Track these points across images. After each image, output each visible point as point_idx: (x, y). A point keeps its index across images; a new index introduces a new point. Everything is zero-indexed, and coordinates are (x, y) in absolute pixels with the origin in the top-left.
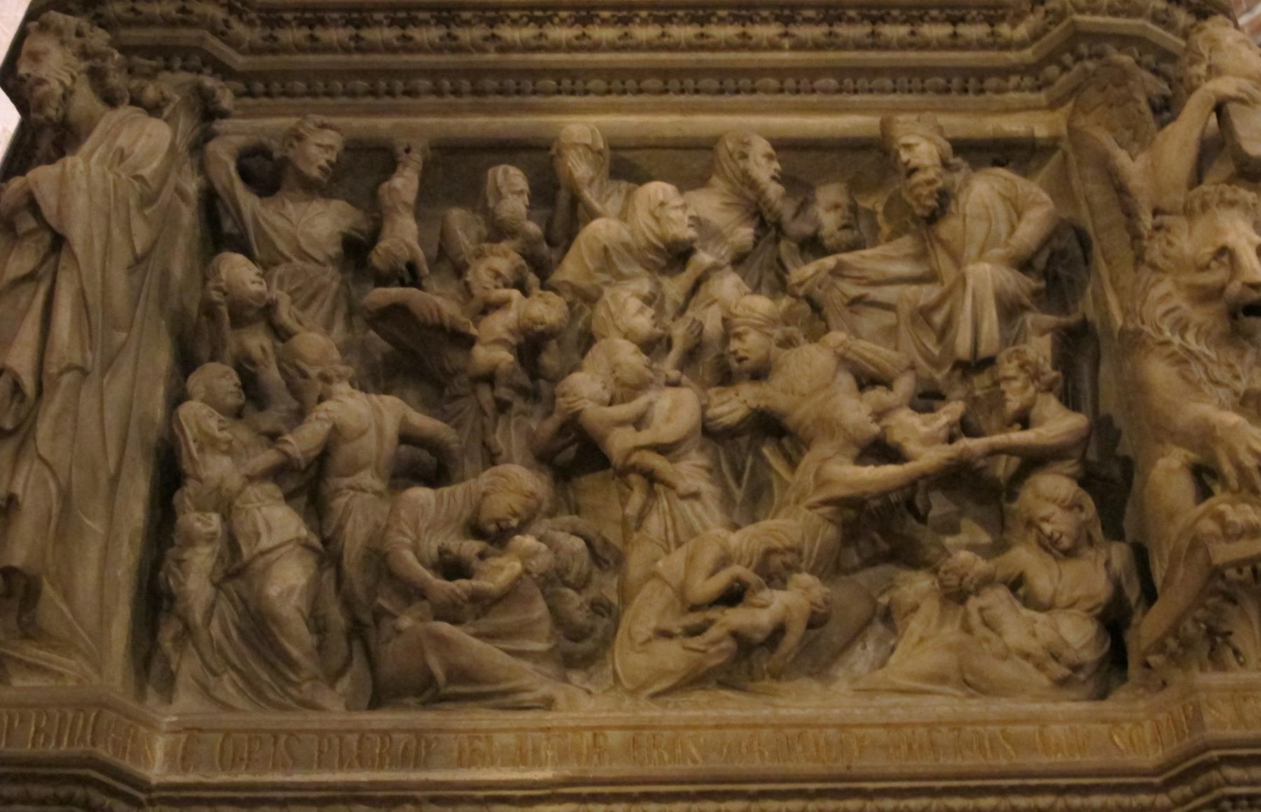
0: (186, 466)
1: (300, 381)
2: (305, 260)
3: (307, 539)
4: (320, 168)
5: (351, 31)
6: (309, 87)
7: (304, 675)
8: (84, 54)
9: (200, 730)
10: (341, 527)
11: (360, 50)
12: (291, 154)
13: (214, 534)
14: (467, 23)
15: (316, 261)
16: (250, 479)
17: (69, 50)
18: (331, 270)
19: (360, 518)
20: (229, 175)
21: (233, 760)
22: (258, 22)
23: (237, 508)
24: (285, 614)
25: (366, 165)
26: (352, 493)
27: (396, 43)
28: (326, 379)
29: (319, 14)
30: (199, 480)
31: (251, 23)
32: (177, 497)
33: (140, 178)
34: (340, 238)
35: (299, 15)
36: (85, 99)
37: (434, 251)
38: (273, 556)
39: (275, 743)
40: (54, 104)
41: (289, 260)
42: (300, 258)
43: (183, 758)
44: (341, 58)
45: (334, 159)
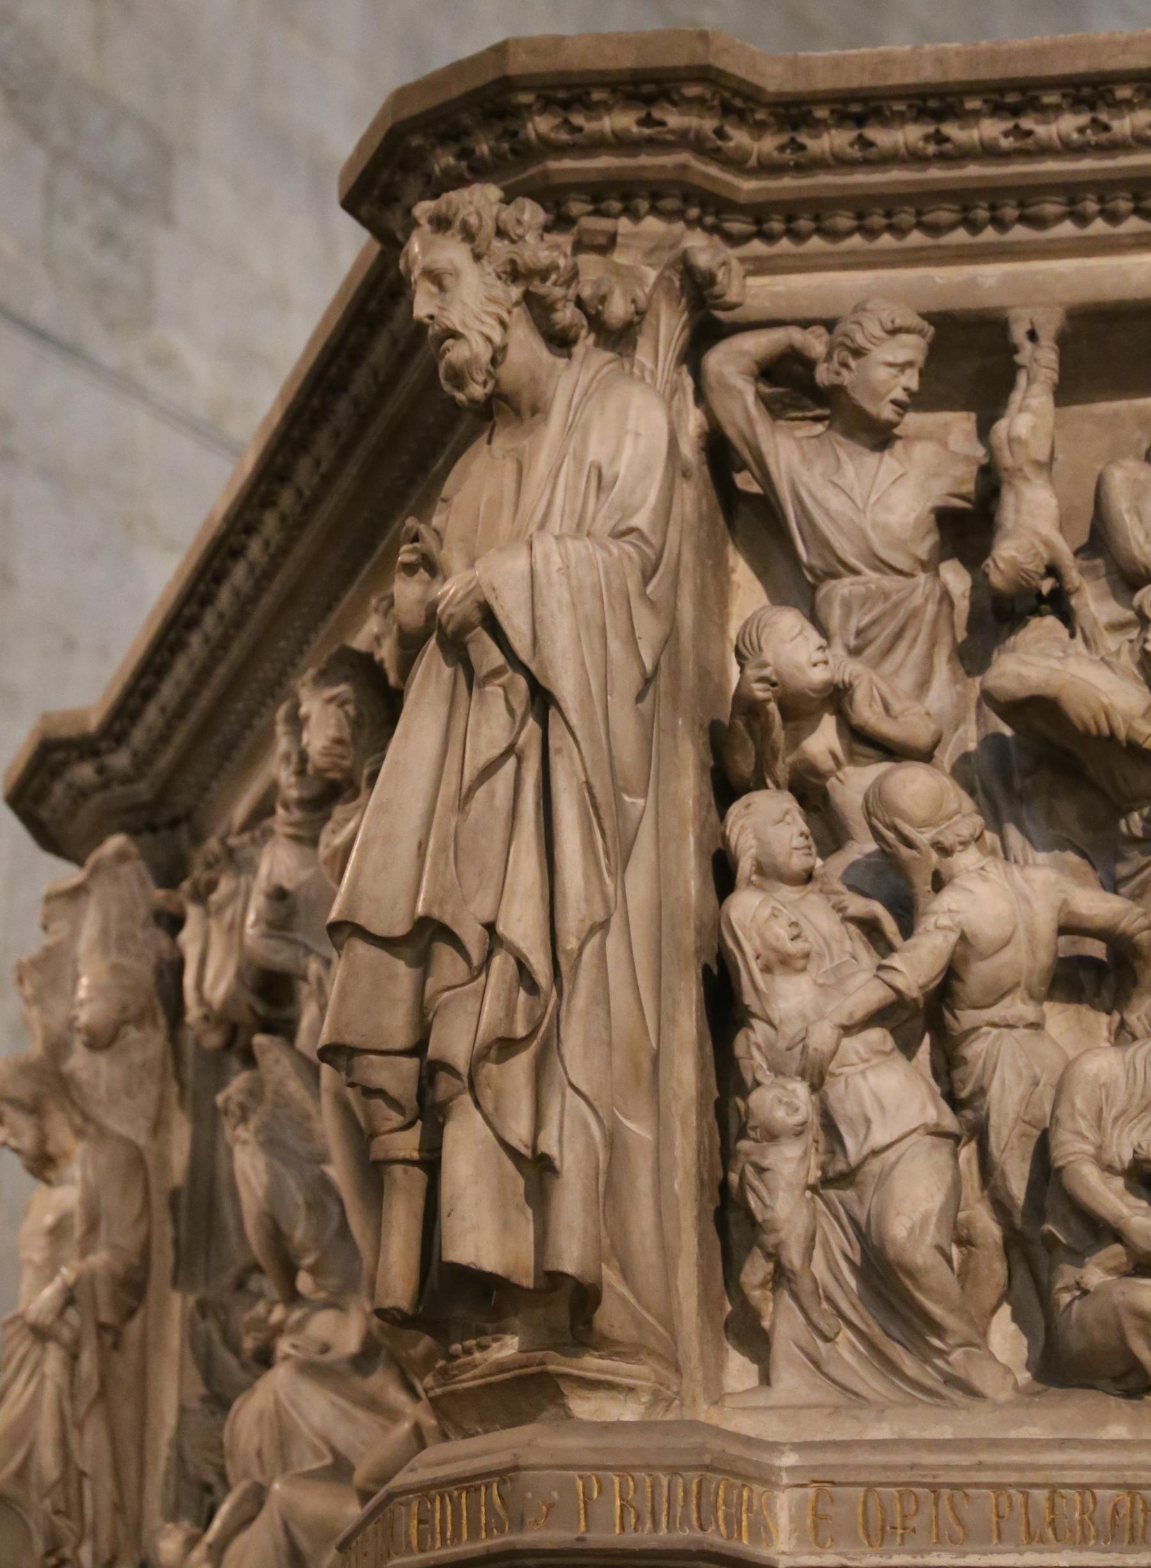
2: (884, 573)
4: (894, 402)
7: (951, 1341)
9: (833, 1483)
12: (846, 378)
13: (804, 1124)
15: (900, 572)
16: (848, 1030)
17: (489, 269)
19: (1010, 1077)
20: (746, 410)
21: (883, 1529)
23: (833, 1075)
24: (920, 1260)
28: (945, 851)
30: (770, 1022)
34: (932, 517)
37: (1084, 539)
38: (891, 1155)
39: (936, 1504)
41: (855, 572)
42: (875, 569)
43: (816, 1527)
45: (914, 385)
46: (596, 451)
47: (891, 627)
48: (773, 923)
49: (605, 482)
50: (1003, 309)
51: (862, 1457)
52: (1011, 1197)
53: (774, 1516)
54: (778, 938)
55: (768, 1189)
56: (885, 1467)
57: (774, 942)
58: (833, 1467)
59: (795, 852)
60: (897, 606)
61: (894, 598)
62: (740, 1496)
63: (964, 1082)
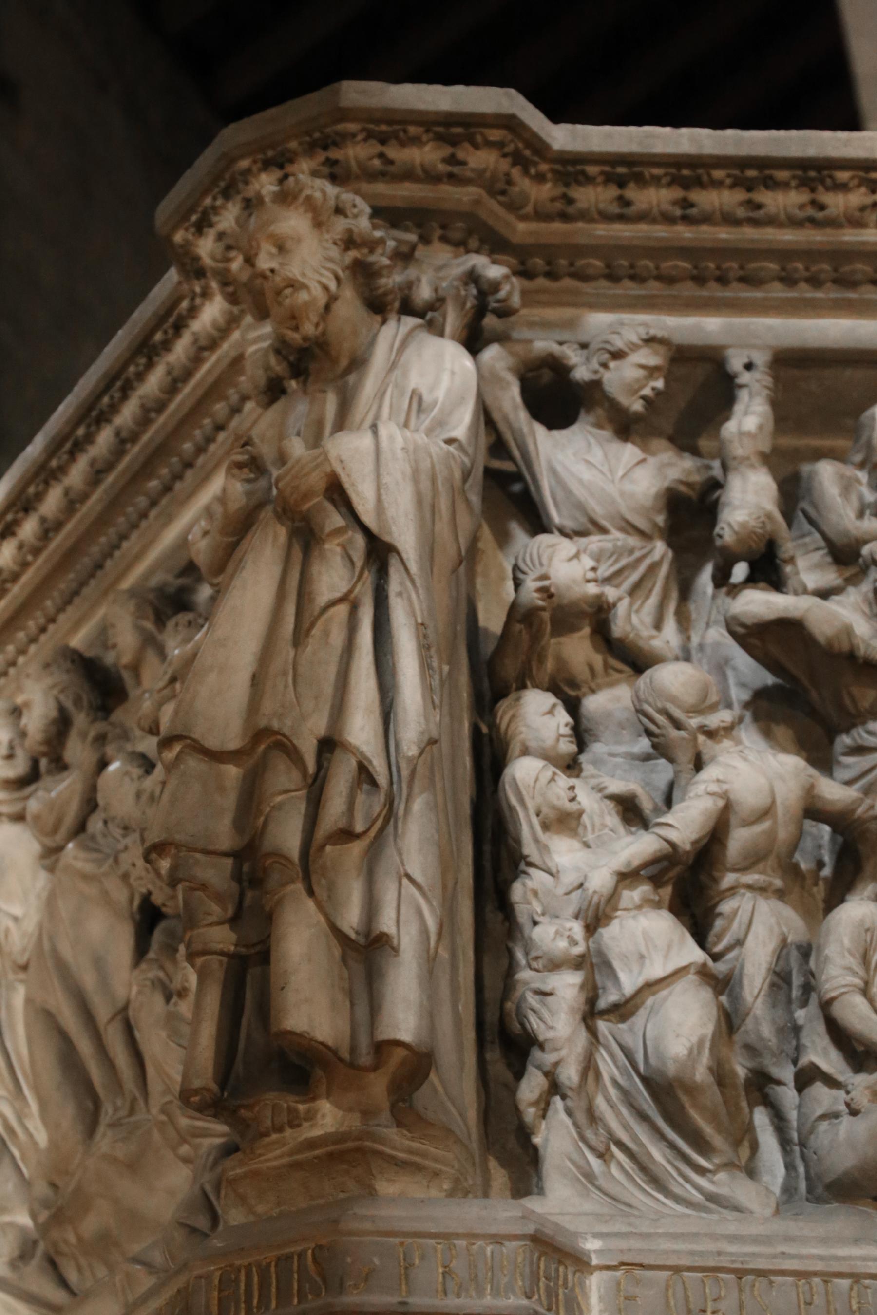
0: (529, 849)
1: (674, 733)
3: (704, 965)
4: (643, 398)
5: (677, 193)
6: (608, 266)
8: (349, 242)
9: (641, 1266)
10: (739, 943)
11: (686, 219)
14: (843, 187)
16: (627, 877)
18: (660, 548)
22: (549, 176)
25: (695, 395)
26: (749, 895)
27: (741, 213)
29: (636, 169)
31: (540, 178)
32: (517, 892)
33: (450, 441)
35: (607, 169)
36: (349, 307)
40: (314, 319)
44: (660, 232)
46: (415, 380)
47: (635, 577)
48: (552, 783)
49: (424, 405)
50: (724, 347)
51: (665, 1245)
52: (761, 1039)
53: (587, 1297)
54: (559, 798)
55: (550, 1011)
56: (692, 1253)
57: (556, 802)
58: (640, 1251)
59: (562, 739)
60: (639, 560)
61: (637, 554)
62: (557, 1270)
63: (719, 937)
